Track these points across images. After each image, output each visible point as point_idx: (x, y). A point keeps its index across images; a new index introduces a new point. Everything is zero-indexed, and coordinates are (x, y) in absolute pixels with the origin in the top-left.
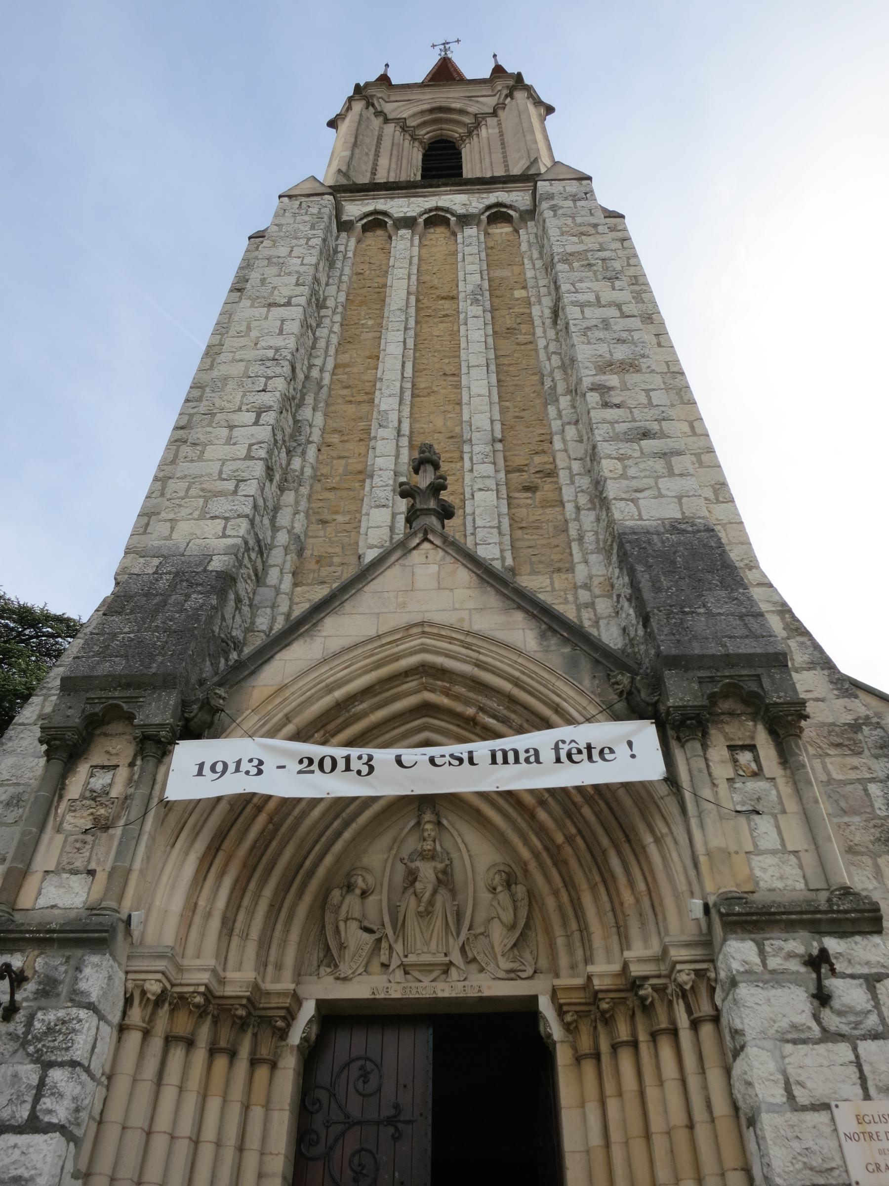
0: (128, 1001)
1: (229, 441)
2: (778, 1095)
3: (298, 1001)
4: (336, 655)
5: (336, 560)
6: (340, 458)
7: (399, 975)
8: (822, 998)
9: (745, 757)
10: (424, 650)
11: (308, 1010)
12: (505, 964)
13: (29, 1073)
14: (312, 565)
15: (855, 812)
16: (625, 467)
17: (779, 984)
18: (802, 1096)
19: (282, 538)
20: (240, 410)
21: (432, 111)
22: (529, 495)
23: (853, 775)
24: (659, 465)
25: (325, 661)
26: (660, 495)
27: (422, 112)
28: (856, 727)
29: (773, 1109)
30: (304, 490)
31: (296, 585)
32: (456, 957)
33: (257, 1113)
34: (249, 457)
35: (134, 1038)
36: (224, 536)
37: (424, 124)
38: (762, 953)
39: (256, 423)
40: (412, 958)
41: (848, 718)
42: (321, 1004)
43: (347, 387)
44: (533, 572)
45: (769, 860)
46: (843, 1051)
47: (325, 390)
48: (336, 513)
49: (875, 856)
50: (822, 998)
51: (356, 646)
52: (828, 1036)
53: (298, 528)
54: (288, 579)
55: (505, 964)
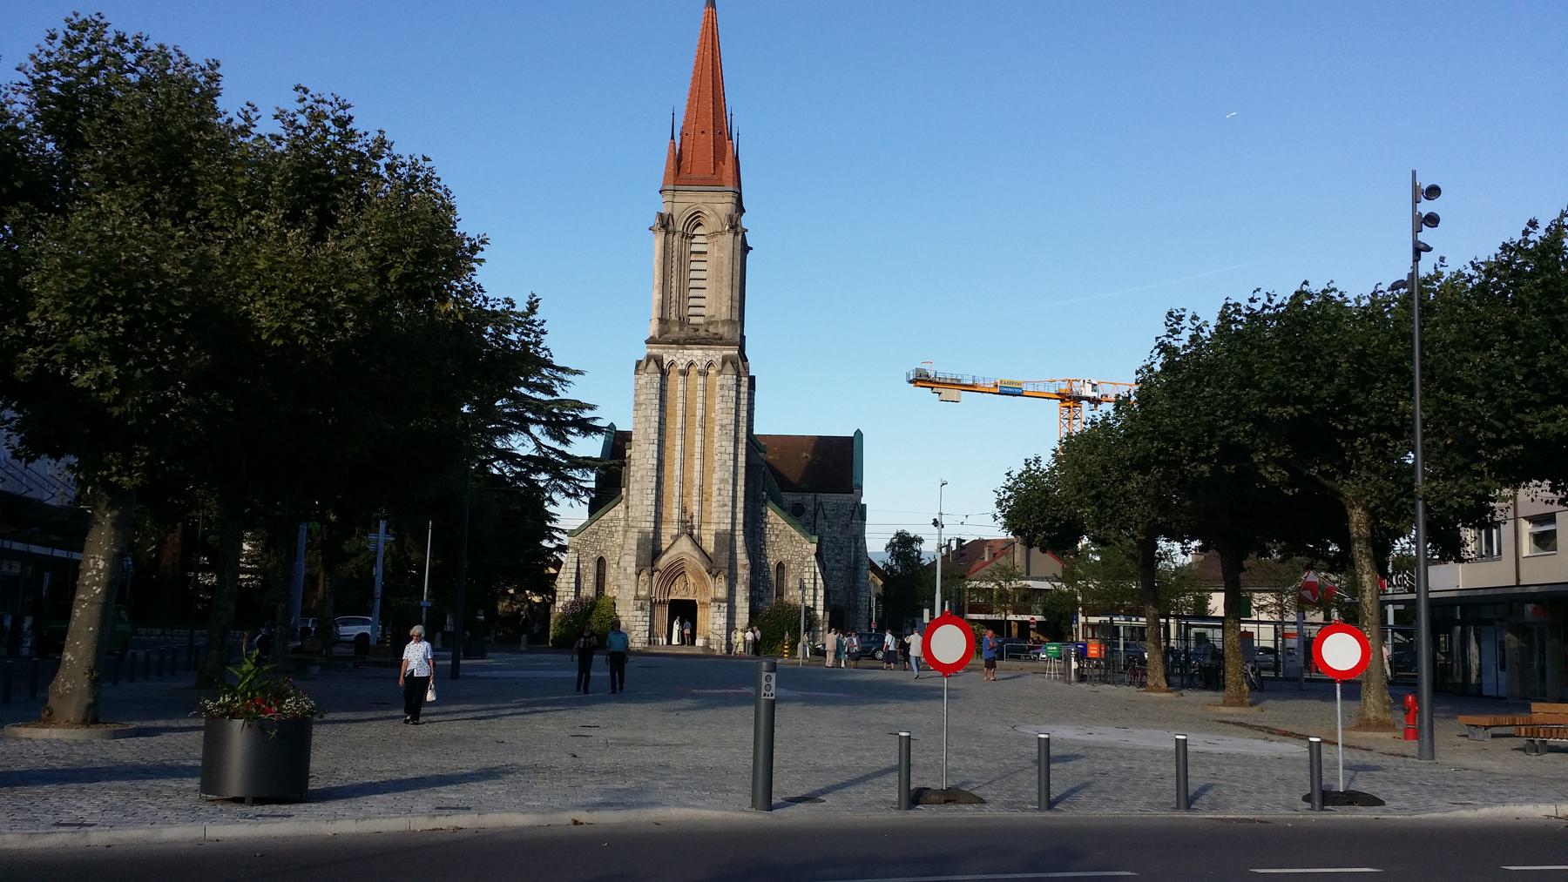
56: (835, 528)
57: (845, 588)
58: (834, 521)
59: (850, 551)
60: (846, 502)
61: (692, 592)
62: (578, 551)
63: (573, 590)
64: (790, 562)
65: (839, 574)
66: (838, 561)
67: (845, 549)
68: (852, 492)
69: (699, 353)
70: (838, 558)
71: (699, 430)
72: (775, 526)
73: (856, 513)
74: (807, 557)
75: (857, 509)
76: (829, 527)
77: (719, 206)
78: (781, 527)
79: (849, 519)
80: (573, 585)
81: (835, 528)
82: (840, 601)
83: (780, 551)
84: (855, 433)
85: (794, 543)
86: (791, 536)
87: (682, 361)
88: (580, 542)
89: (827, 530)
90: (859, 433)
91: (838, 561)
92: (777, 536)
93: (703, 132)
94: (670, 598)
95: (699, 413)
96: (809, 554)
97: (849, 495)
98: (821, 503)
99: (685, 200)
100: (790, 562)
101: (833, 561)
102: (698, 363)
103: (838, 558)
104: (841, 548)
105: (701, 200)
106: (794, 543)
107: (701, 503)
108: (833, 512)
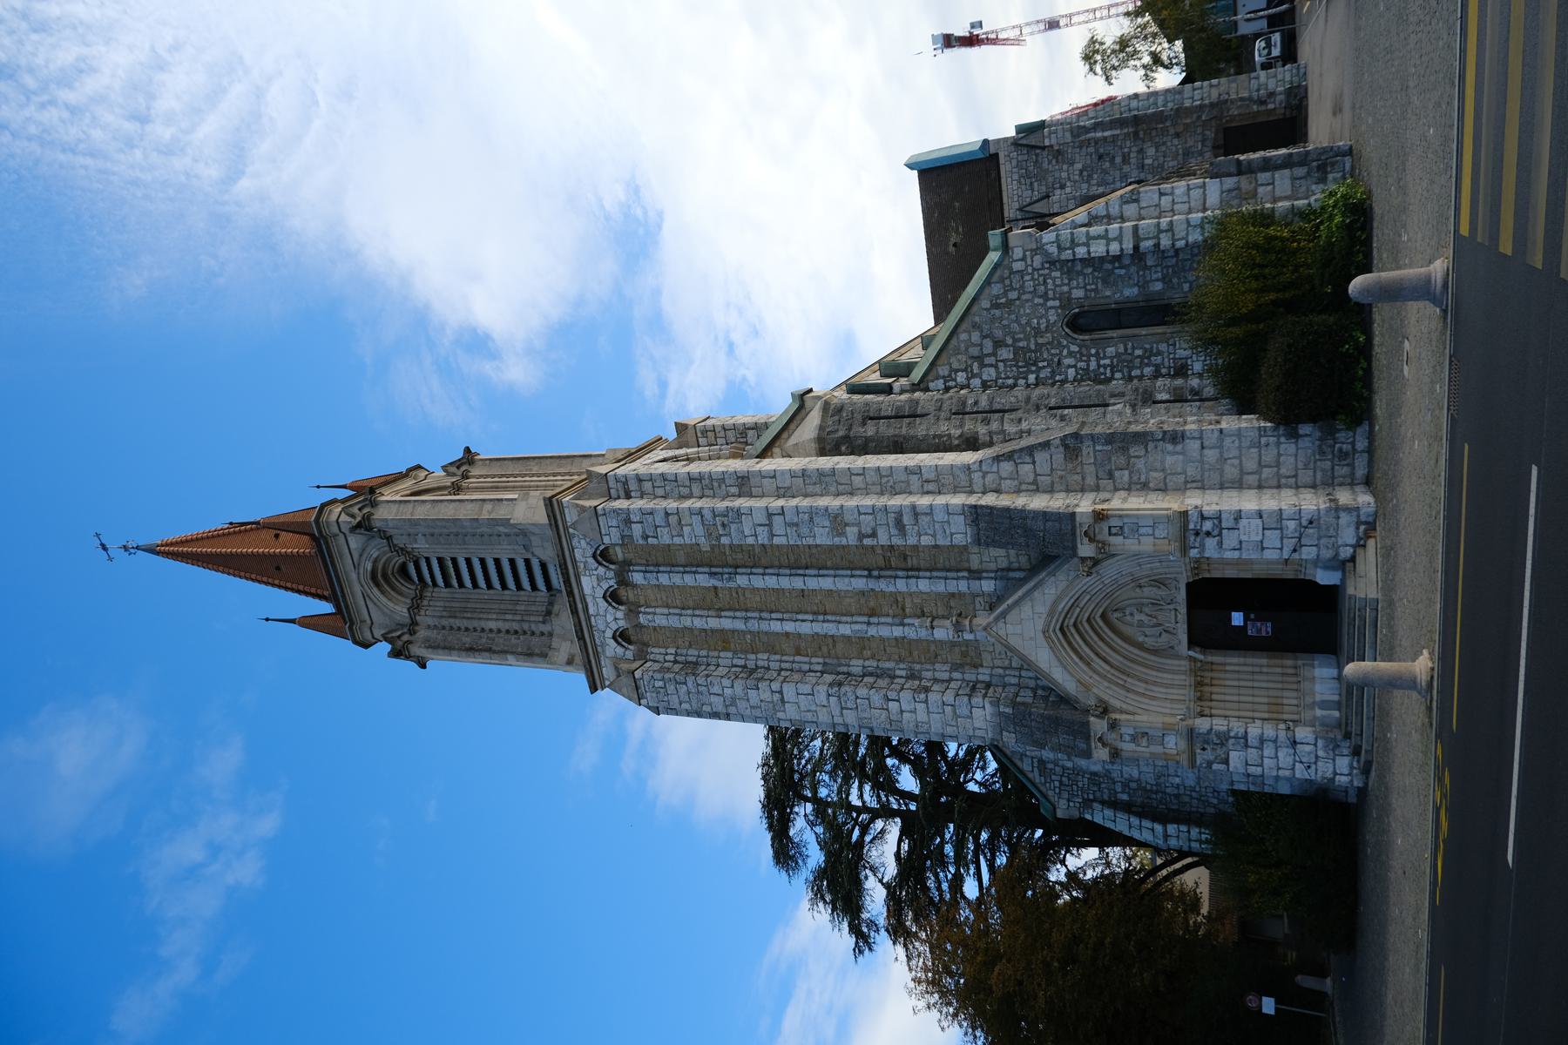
0: (1203, 716)
1: (914, 711)
2: (1237, 553)
3: (1191, 658)
4: (1061, 663)
5: (963, 649)
6: (885, 650)
7: (1178, 625)
8: (1208, 534)
9: (1114, 531)
10: (1054, 631)
11: (1191, 653)
12: (1174, 591)
13: (1231, 741)
14: (968, 660)
15: (1110, 459)
16: (926, 534)
17: (1204, 545)
18: (1238, 547)
19: (956, 675)
20: (887, 709)
21: (377, 585)
22: (909, 558)
23: (1092, 454)
24: (924, 520)
25: (1065, 668)
26: (948, 522)
27: (383, 592)
28: (1066, 447)
29: (1241, 554)
30: (917, 667)
31: (982, 666)
32: (1171, 607)
33: (1228, 668)
34: (926, 702)
35: (1214, 712)
36: (984, 707)
37: (400, 593)
38: (1195, 548)
39: (898, 701)
40: (1173, 621)
41: (1061, 449)
42: (1189, 649)
43: (820, 648)
44: (968, 561)
45: (1157, 532)
46: (1224, 532)
47: (827, 660)
48: (929, 650)
49: (1130, 457)
50: (1208, 534)
51: (1056, 656)
52: (1220, 535)
53: (947, 667)
54: (980, 670)
55: (1174, 591)
56: (1064, 175)
57: (1177, 135)
58: (1050, 179)
59: (1105, 138)
60: (1014, 163)
61: (1163, 592)
62: (1087, 804)
63: (1184, 828)
64: (1066, 301)
65: (1151, 151)
66: (1126, 159)
67: (1101, 150)
68: (997, 155)
69: (585, 581)
70: (1118, 160)
71: (742, 581)
72: (975, 351)
73: (1032, 141)
74: (1047, 254)
75: (1024, 142)
76: (1063, 187)
77: (353, 545)
78: (976, 337)
79: (1045, 153)
80: (1172, 828)
81: (1064, 175)
82: (1203, 141)
83: (1038, 332)
84: (912, 168)
85: (1013, 295)
86: (996, 306)
87: (610, 618)
88: (1065, 795)
89: (1068, 190)
90: (910, 166)
91: (1126, 159)
92: (998, 344)
93: (278, 568)
94: (1183, 648)
95: (703, 580)
96: (1039, 249)
97: (1002, 160)
98: (1021, 209)
99: (363, 603)
100: (1066, 301)
101: (1126, 168)
102: (605, 586)
103: (1118, 160)
104: (1100, 157)
105: (354, 576)
106: (1013, 295)
107: (913, 571)
108: (1036, 184)
